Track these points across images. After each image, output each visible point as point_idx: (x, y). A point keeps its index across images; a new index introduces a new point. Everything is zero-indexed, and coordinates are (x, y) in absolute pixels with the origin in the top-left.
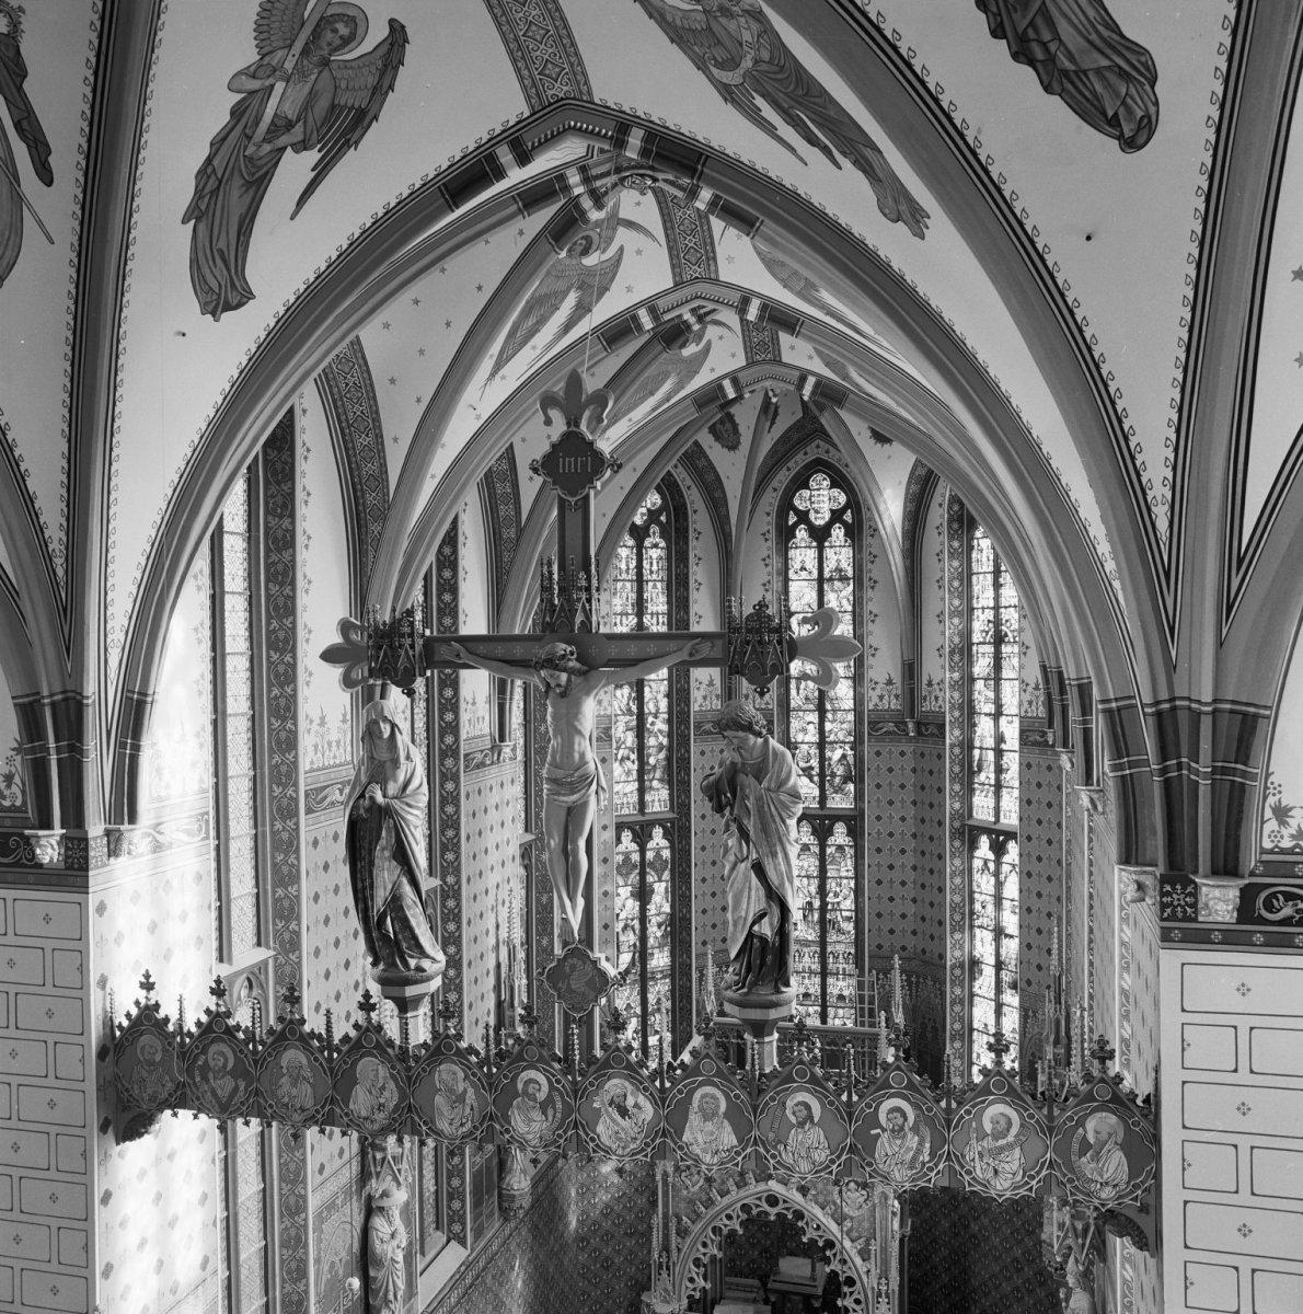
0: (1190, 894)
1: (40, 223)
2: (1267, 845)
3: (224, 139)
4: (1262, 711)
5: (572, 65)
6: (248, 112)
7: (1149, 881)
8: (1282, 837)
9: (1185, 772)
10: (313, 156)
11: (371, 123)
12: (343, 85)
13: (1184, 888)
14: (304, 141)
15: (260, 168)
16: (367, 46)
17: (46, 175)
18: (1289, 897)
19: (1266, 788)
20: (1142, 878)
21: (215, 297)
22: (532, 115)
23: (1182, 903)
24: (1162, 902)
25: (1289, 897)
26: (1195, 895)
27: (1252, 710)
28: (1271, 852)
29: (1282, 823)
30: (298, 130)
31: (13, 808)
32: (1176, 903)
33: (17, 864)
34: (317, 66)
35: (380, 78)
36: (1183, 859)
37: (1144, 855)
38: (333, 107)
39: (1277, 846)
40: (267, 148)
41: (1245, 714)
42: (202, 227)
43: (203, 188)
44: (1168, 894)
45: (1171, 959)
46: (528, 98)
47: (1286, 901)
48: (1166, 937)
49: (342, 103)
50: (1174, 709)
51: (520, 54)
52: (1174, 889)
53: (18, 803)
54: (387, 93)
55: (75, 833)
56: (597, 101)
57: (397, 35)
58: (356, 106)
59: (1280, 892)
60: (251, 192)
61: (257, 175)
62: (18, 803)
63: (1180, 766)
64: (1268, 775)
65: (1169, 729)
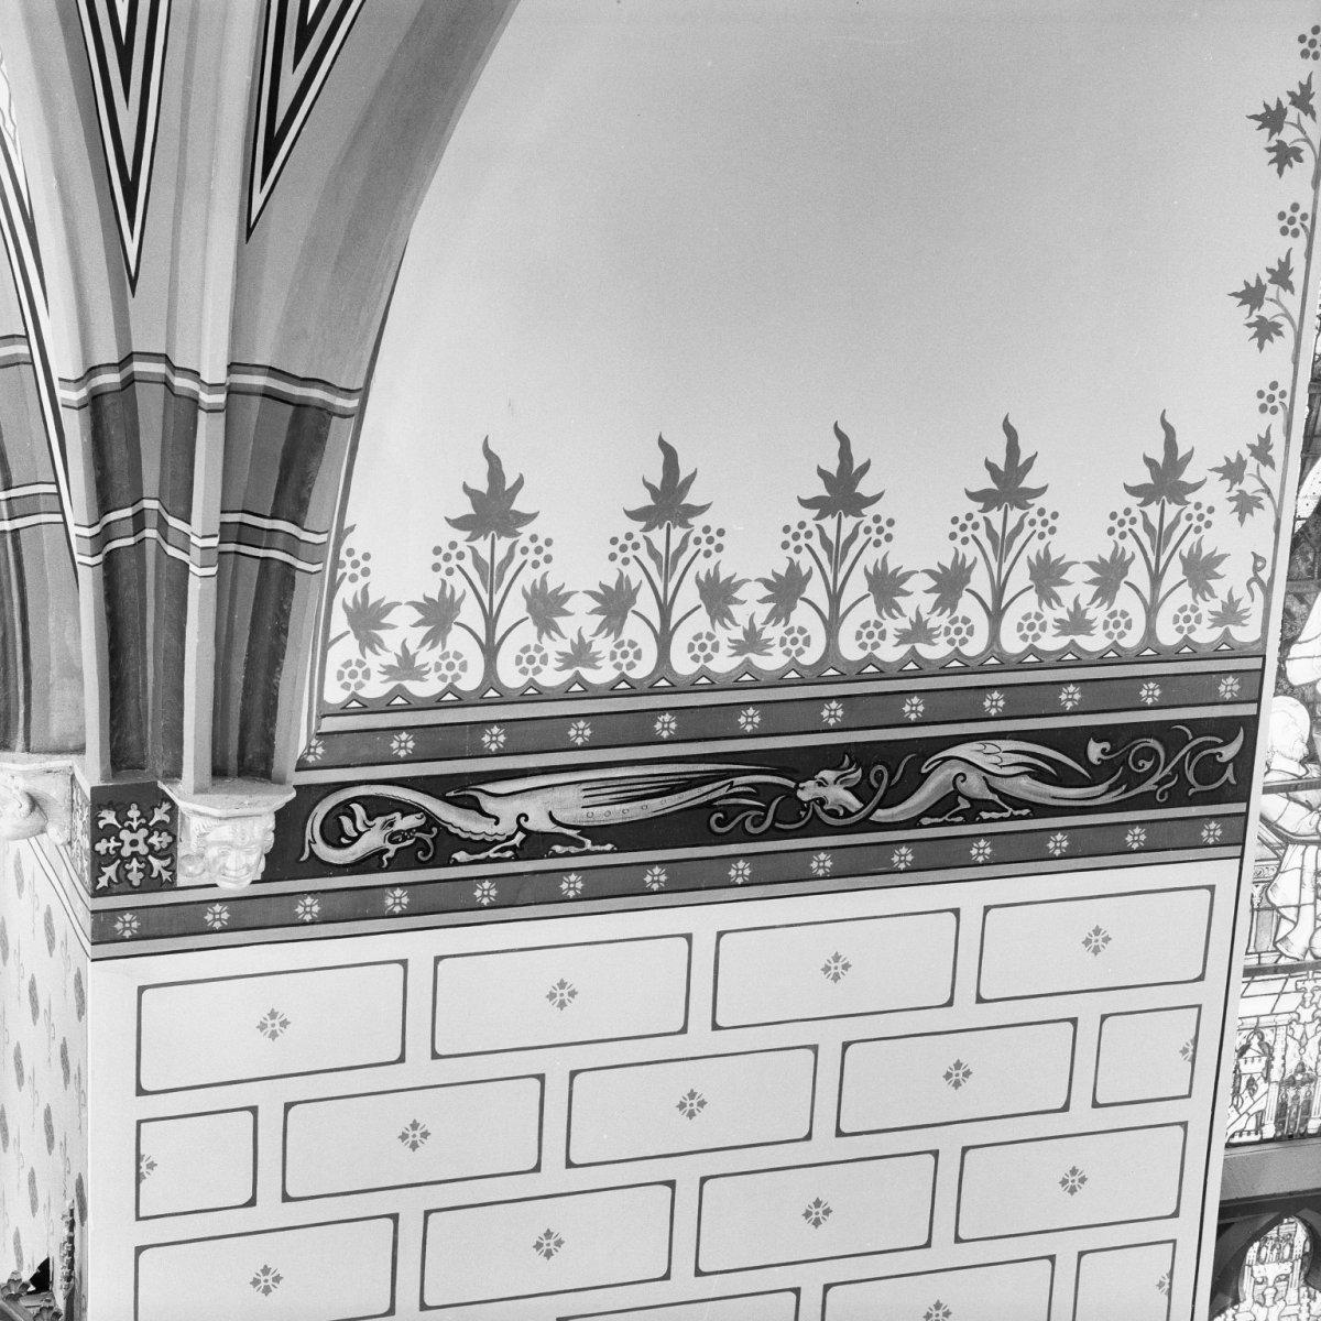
0: (161, 827)
2: (335, 694)
4: (340, 402)
7: (54, 790)
8: (367, 674)
9: (151, 533)
13: (146, 815)
18: (377, 807)
19: (337, 563)
20: (41, 786)
23: (142, 849)
24: (95, 853)
25: (377, 807)
26: (170, 828)
27: (316, 394)
28: (344, 711)
29: (369, 642)
32: (126, 851)
36: (142, 743)
37: (46, 723)
39: (355, 697)
41: (301, 406)
44: (110, 832)
45: (113, 980)
47: (370, 817)
48: (104, 932)
50: (129, 382)
52: (122, 817)
59: (355, 800)
63: (139, 521)
64: (342, 534)
65: (115, 432)
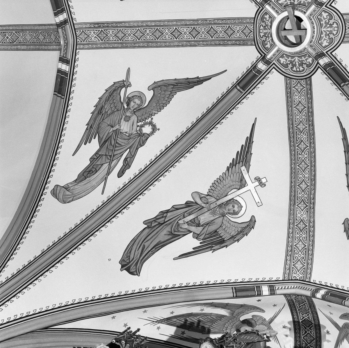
3: (177, 209)
5: (308, 264)
6: (191, 208)
10: (197, 243)
11: (224, 246)
12: (224, 227)
14: (198, 235)
15: (179, 231)
16: (239, 220)
17: (121, 174)
21: (128, 261)
22: (283, 280)
30: (200, 228)
34: (220, 214)
35: (236, 235)
38: (216, 231)
40: (186, 226)
42: (147, 231)
43: (158, 219)
46: (285, 273)
49: (219, 233)
51: (290, 253)
54: (236, 241)
56: (312, 281)
57: (251, 224)
58: (223, 237)
60: (170, 237)
61: (176, 233)
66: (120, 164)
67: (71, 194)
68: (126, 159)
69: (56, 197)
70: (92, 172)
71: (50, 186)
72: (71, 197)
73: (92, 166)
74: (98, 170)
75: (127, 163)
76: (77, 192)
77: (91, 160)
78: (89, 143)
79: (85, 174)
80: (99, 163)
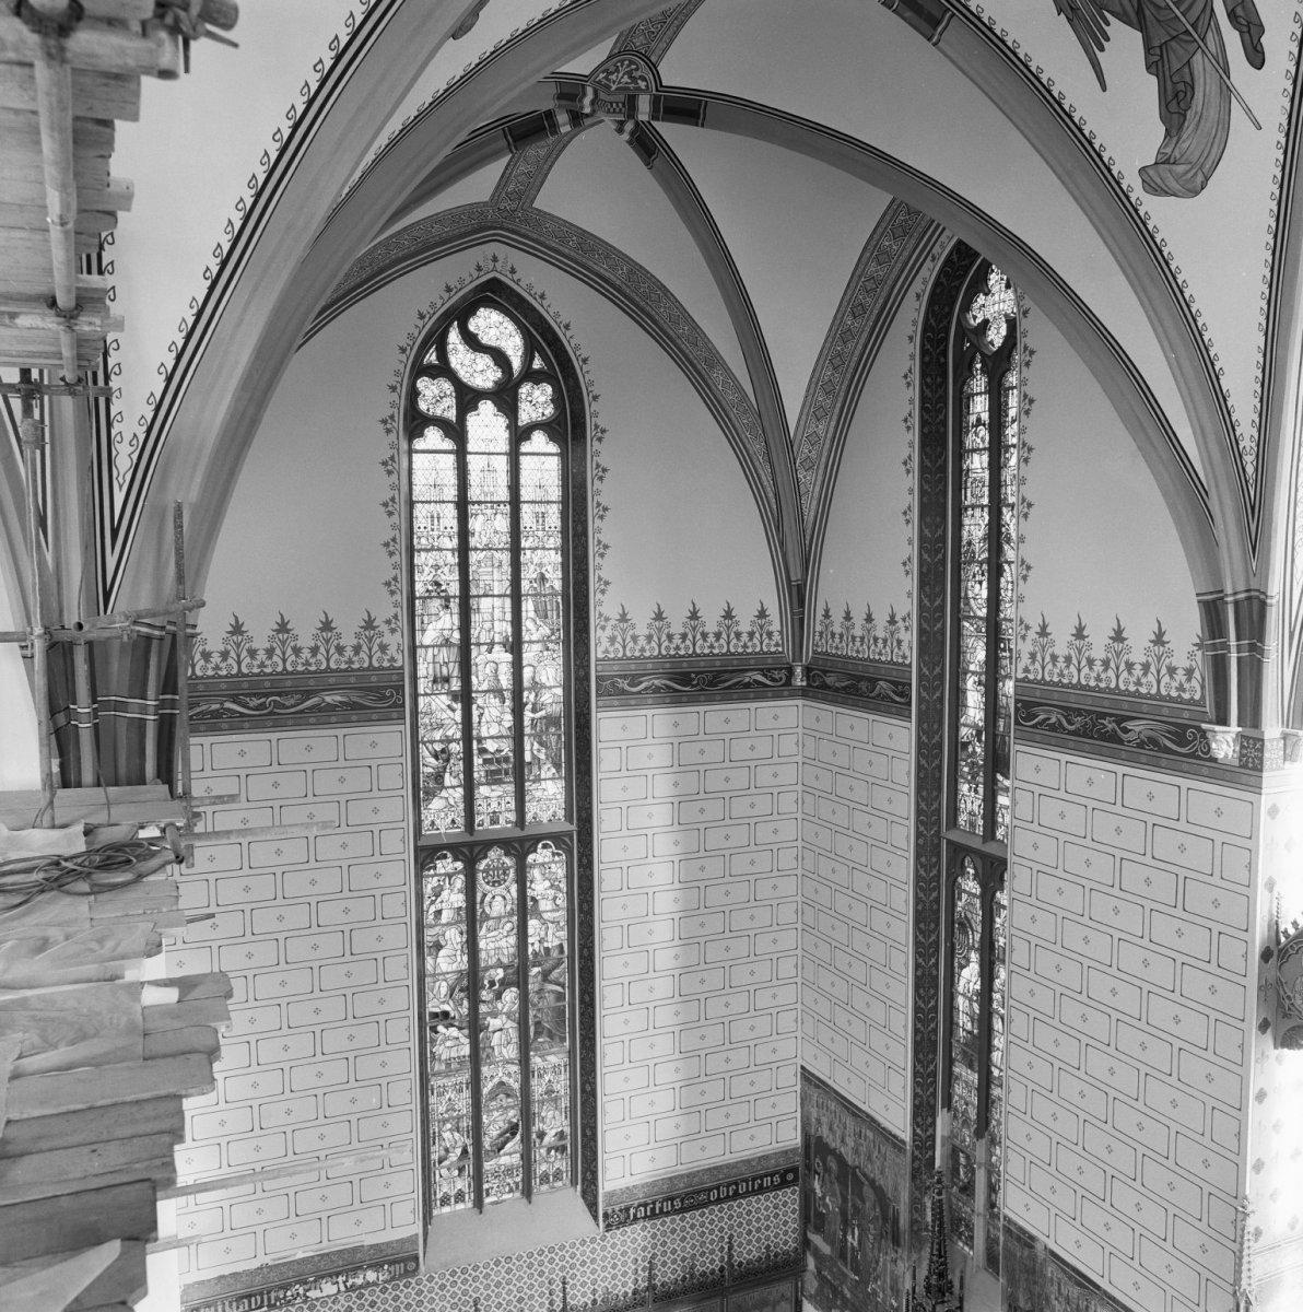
1: (1248, 111)
17: (1256, 57)
31: (1191, 702)
33: (1193, 755)
53: (1197, 697)
55: (1250, 732)
62: (1197, 697)
66: (1232, 40)
67: (1188, 167)
68: (1232, 16)
69: (1167, 194)
70: (1181, 95)
71: (1132, 182)
72: (1196, 174)
73: (1169, 82)
74: (1192, 79)
75: (1244, 22)
76: (1197, 154)
77: (1154, 69)
78: (1108, 39)
79: (1173, 107)
80: (1176, 66)
